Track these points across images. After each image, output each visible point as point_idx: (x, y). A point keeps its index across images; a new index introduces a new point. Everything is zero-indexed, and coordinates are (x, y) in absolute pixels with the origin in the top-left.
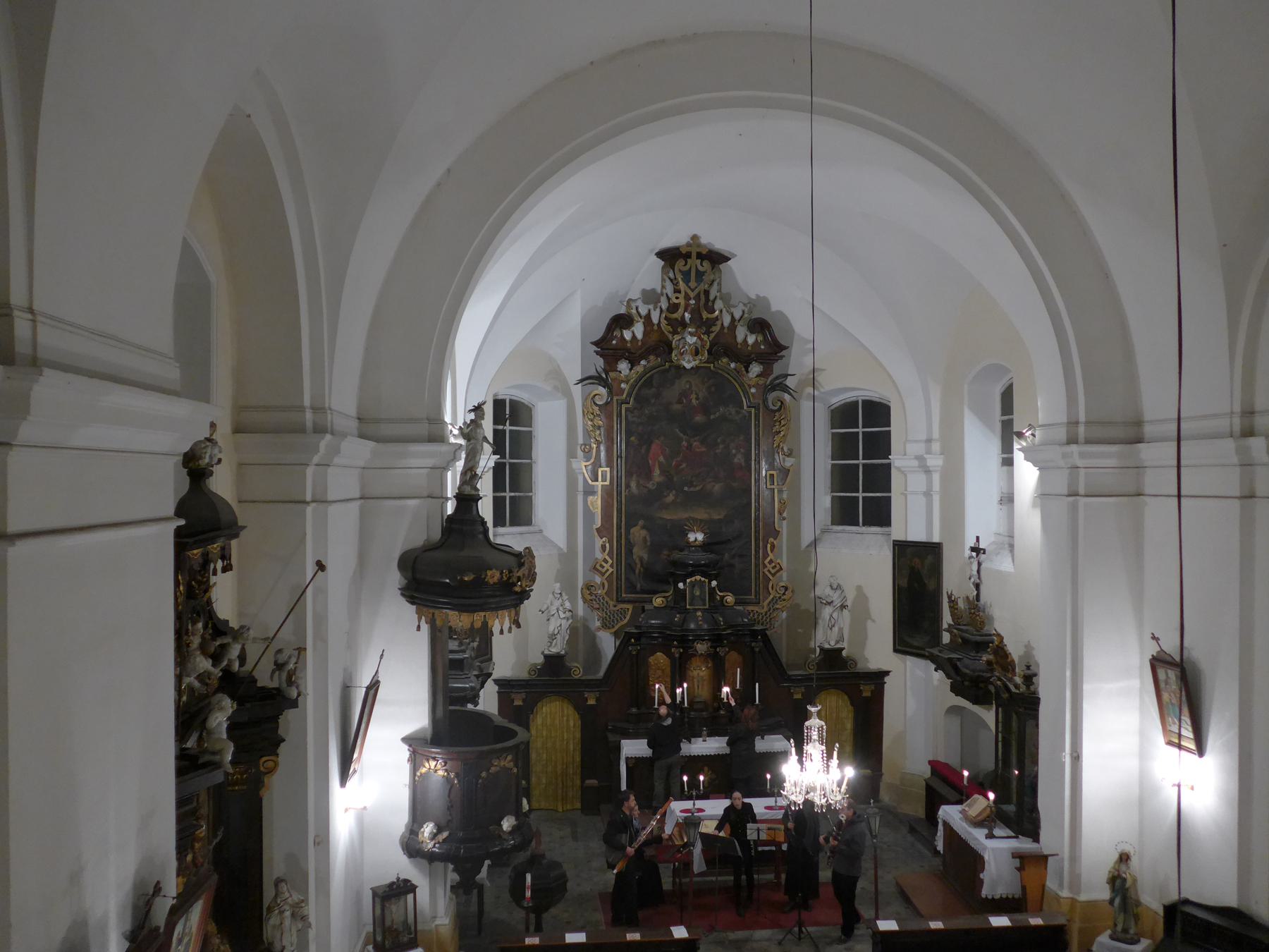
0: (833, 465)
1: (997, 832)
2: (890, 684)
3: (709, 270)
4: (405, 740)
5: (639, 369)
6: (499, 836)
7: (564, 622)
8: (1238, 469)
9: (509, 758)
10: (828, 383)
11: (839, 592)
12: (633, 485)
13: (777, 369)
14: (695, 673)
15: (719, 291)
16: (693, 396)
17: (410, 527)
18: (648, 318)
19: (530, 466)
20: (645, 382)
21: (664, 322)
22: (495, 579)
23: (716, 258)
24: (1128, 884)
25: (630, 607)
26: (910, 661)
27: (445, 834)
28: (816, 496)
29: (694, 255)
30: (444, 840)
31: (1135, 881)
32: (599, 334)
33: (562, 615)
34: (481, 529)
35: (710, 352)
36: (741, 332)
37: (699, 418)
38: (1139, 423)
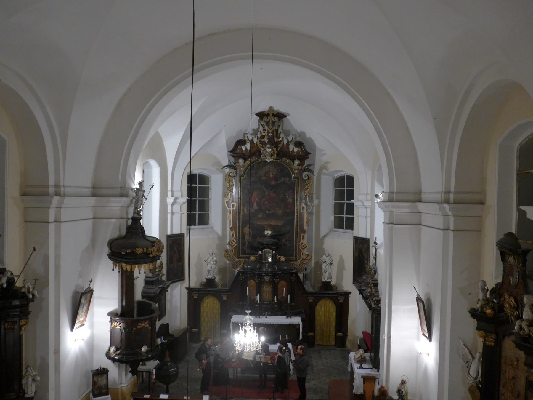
0: (335, 203)
1: (363, 366)
3: (278, 121)
4: (109, 314)
5: (248, 162)
6: (141, 353)
7: (213, 266)
8: (442, 217)
9: (147, 322)
10: (332, 168)
11: (329, 257)
12: (245, 210)
13: (307, 162)
15: (282, 129)
16: (271, 173)
17: (113, 229)
18: (252, 141)
19: (208, 201)
20: (251, 167)
21: (259, 143)
22: (140, 252)
23: (281, 116)
24: (404, 393)
25: (243, 260)
27: (119, 351)
28: (327, 216)
29: (271, 115)
30: (119, 354)
31: (407, 393)
32: (231, 148)
33: (212, 263)
34: (140, 231)
35: (277, 155)
36: (291, 147)
37: (273, 183)
38: (420, 193)
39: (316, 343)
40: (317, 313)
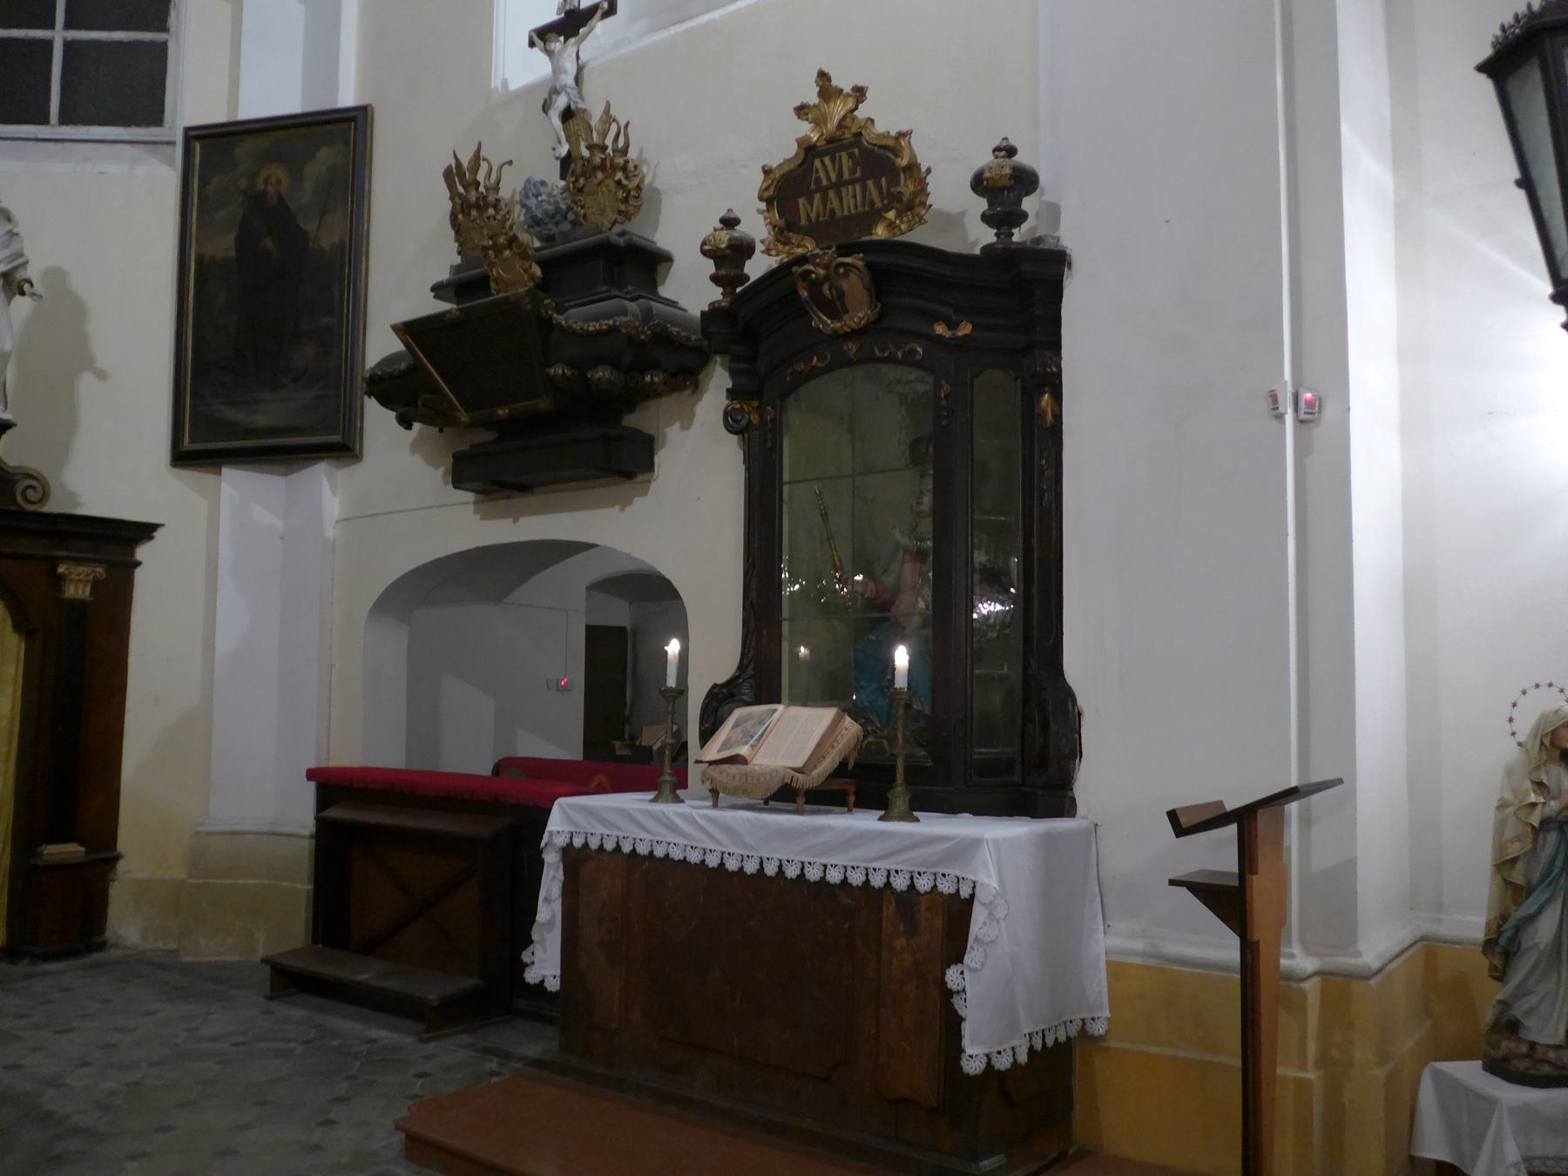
2: (156, 574)
26: (234, 483)
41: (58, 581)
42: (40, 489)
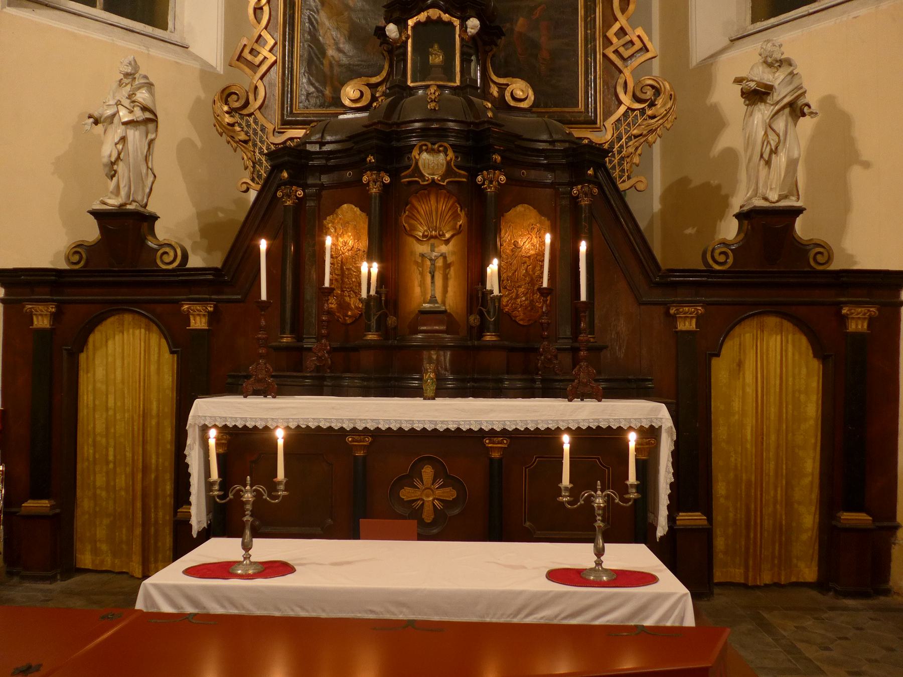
7: (134, 135)
14: (422, 248)
33: (124, 115)
39: (719, 576)
40: (717, 405)
41: (843, 320)
42: (826, 254)
